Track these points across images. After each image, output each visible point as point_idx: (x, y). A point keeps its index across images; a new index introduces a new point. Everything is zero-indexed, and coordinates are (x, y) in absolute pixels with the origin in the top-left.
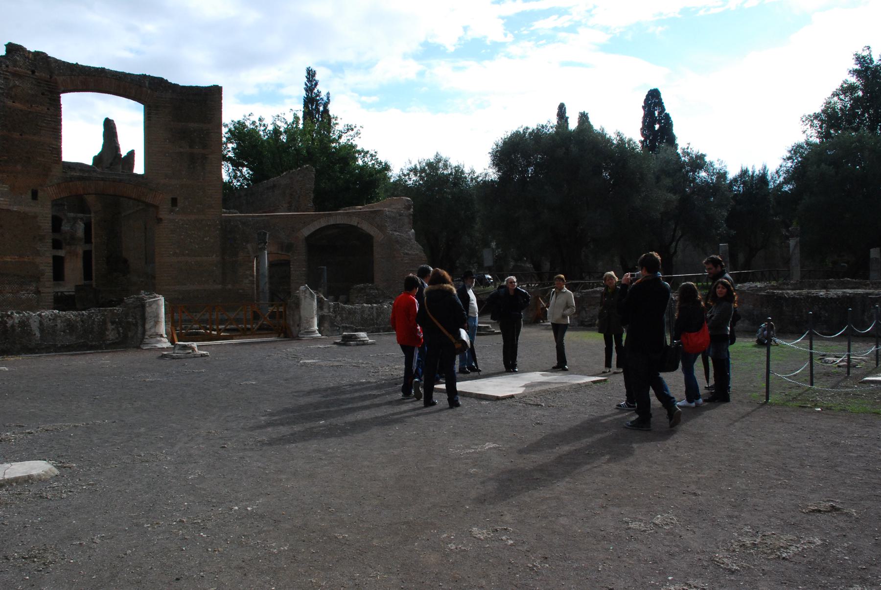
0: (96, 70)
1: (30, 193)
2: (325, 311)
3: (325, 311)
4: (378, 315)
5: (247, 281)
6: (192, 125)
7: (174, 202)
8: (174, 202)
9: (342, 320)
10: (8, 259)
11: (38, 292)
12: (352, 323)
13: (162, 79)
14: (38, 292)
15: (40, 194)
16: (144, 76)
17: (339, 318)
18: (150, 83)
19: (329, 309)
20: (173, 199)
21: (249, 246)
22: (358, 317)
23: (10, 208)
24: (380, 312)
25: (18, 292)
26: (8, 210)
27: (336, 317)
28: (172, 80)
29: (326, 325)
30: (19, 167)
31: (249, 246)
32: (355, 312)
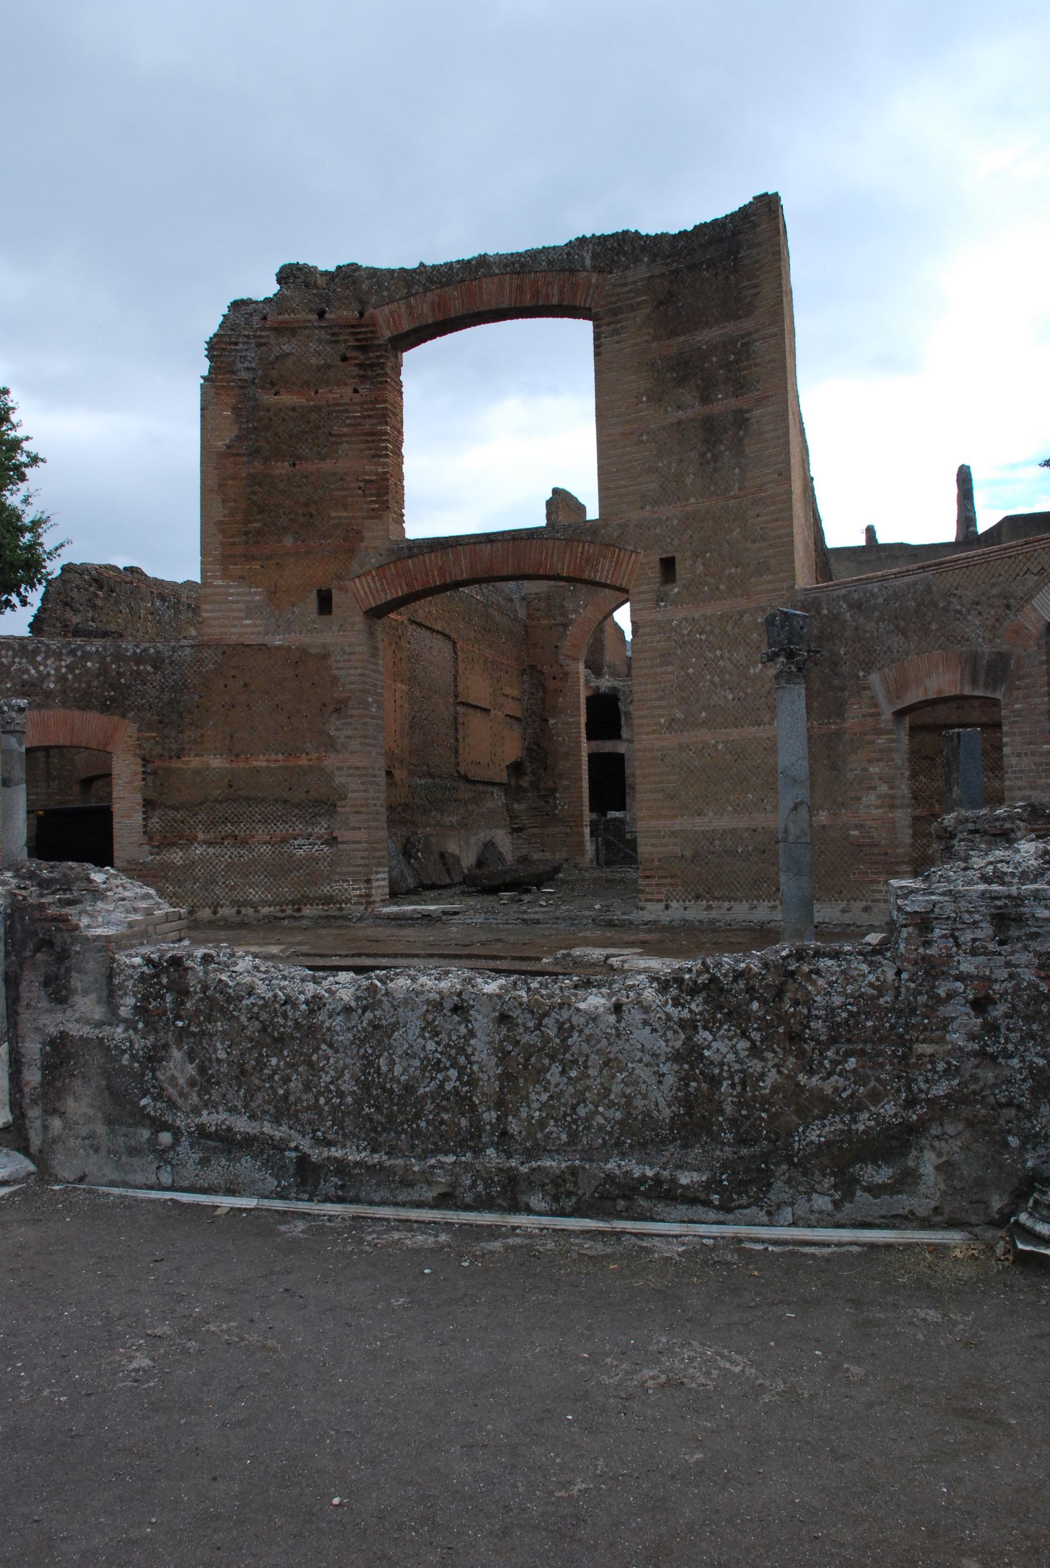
0: (465, 264)
1: (313, 597)
2: (83, 1014)
3: (83, 1014)
4: (518, 1070)
5: (871, 798)
6: (708, 336)
7: (668, 566)
8: (668, 566)
9: (205, 1080)
10: (260, 763)
11: (332, 841)
12: (283, 1110)
13: (625, 233)
14: (332, 841)
15: (337, 598)
16: (582, 241)
17: (178, 1067)
18: (595, 256)
19: (110, 997)
20: (662, 560)
21: (875, 679)
22: (339, 1069)
23: (268, 640)
24: (533, 1047)
25: (284, 840)
26: (263, 647)
27: (154, 1058)
28: (650, 226)
29: (81, 1104)
30: (288, 541)
31: (875, 679)
32: (310, 1032)
